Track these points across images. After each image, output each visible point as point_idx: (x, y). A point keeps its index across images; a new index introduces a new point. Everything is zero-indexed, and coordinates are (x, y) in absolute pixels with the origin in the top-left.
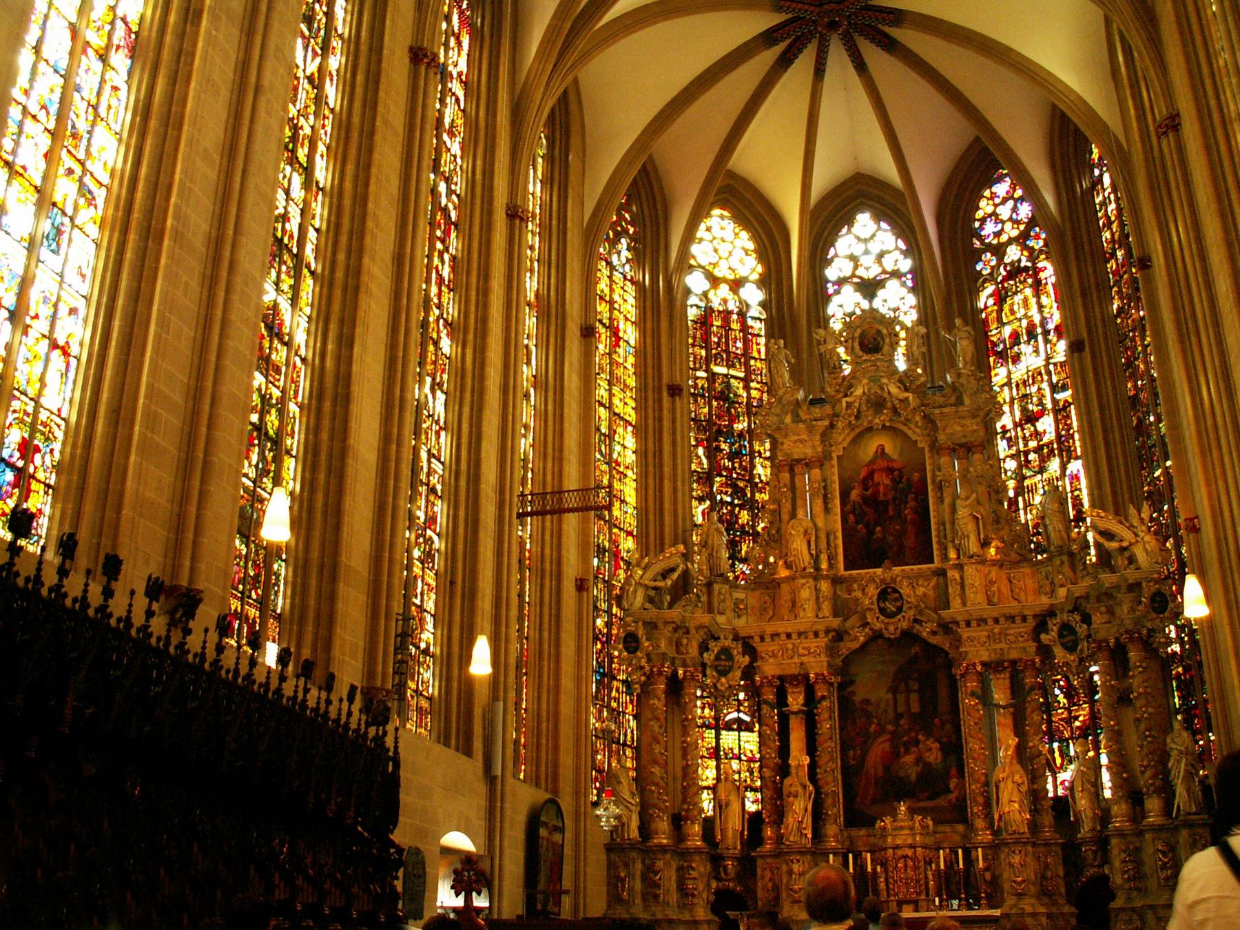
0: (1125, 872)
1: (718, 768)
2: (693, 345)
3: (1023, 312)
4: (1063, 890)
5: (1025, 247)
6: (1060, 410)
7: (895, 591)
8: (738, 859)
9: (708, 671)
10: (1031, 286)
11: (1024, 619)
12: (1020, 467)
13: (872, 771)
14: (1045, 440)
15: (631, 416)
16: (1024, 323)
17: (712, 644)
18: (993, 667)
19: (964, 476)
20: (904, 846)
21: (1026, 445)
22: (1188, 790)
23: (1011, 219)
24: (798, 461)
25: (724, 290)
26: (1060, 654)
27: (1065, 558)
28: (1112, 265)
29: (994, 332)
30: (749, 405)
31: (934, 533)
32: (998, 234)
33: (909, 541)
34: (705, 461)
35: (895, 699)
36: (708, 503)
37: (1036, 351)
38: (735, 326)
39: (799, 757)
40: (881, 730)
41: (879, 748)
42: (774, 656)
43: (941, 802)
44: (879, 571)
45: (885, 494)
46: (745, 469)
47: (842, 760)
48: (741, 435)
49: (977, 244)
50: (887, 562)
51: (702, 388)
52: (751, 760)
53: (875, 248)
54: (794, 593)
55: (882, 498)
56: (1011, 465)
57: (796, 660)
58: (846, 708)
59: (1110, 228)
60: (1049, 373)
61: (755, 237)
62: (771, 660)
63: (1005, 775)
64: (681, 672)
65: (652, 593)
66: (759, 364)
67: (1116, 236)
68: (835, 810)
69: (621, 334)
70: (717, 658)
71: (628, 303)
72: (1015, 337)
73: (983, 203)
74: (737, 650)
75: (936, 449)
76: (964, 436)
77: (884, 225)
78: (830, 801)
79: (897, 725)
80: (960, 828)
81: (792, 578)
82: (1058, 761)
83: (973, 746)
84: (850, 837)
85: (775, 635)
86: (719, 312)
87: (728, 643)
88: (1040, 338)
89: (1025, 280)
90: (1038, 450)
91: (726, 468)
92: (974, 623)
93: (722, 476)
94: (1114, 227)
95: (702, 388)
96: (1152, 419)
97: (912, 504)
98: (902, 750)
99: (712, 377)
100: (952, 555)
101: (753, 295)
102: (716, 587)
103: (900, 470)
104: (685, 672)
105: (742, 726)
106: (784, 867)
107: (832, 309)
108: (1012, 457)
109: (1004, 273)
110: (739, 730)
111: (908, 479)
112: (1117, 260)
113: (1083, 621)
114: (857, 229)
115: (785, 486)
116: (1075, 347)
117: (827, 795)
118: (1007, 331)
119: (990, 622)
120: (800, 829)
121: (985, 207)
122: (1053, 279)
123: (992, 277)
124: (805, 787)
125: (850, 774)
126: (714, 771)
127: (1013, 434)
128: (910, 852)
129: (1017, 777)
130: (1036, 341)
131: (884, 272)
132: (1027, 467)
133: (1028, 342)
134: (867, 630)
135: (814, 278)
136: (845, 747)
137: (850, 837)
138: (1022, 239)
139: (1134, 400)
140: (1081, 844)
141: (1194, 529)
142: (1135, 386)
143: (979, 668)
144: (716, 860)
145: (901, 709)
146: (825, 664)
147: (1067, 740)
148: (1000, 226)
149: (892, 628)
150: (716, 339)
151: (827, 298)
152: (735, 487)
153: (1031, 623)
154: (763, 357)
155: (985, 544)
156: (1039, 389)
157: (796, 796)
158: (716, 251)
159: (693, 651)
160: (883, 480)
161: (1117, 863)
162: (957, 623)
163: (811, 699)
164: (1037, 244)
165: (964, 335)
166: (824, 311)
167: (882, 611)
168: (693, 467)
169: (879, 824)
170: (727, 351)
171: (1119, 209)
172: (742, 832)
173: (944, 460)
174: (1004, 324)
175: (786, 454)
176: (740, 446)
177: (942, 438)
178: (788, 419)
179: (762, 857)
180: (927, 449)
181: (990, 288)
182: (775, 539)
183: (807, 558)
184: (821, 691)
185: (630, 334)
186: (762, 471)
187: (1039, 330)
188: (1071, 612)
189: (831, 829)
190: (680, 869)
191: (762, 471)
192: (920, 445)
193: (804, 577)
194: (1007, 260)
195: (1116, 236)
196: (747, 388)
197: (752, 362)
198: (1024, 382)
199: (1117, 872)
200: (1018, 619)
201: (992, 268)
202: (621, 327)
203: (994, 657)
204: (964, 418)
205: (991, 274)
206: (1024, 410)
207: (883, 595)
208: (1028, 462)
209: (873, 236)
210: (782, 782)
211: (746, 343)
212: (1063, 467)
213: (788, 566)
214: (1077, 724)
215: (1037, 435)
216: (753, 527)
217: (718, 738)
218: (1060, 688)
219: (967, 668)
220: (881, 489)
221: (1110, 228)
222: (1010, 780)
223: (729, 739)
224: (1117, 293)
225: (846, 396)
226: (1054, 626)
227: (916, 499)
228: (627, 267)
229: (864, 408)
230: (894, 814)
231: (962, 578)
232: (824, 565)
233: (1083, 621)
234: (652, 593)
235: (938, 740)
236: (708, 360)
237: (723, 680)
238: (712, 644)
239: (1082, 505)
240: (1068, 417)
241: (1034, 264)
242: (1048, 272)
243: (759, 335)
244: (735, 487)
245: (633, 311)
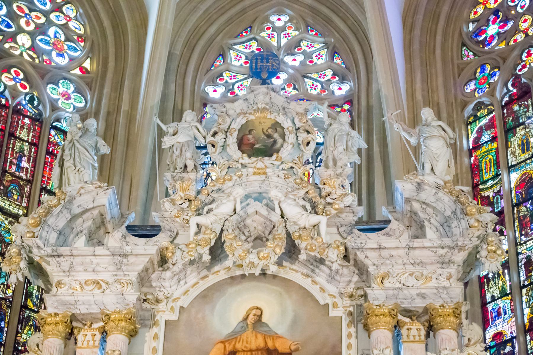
76: (423, 296)
148: (510, 24)
175: (64, 304)
192: (333, 313)
204: (421, 263)
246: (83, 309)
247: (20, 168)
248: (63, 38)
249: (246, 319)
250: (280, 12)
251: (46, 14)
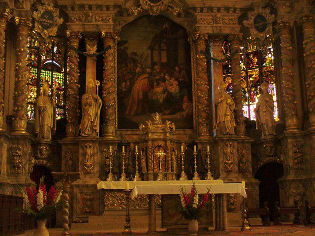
0: (295, 159)
1: (38, 92)
4: (251, 169)
8: (50, 145)
11: (235, 11)
13: (136, 96)
17: (39, 7)
18: (213, 38)
20: (160, 139)
35: (152, 53)
39: (91, 82)
40: (143, 73)
41: (141, 83)
42: (80, 20)
43: (178, 116)
47: (118, 88)
52: (58, 89)
57: (93, 23)
58: (123, 58)
62: (77, 22)
63: (222, 99)
64: (17, 20)
68: (113, 117)
70: (43, 16)
74: (56, 13)
78: (110, 111)
79: (152, 68)
80: (189, 132)
83: (199, 82)
84: (121, 134)
87: (50, 8)
98: (155, 84)
104: (20, 21)
105: (54, 69)
106: (81, 151)
110: (52, 71)
113: (271, 13)
117: (109, 107)
119: (215, 10)
120: (92, 127)
124: (96, 100)
125: (122, 97)
126: (35, 94)
128: (162, 144)
129: (229, 101)
134: (139, 9)
136: (120, 80)
137: (121, 134)
140: (262, 143)
143: (206, 37)
144: (35, 145)
145: (155, 60)
146: (112, 27)
149: (155, 9)
153: (238, 13)
157: (90, 106)
161: (291, 154)
162: (194, 9)
169: (142, 126)
172: (53, 128)
179: (66, 144)
184: (109, 43)
188: (265, 7)
189: (111, 128)
190: (10, 149)
199: (289, 158)
203: (215, 31)
210: (80, 99)
214: (251, 79)
217: (39, 74)
218: (242, 60)
219: (199, 37)
222: (225, 102)
223: (46, 75)
230: (153, 121)
235: (177, 80)
237: (46, 31)
238: (39, 7)
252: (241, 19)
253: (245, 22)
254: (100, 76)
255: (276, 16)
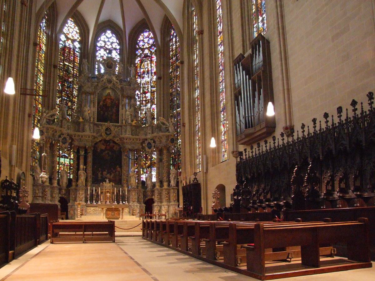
2: (60, 55)
3: (147, 66)
5: (149, 50)
6: (152, 92)
7: (110, 129)
9: (60, 143)
10: (150, 61)
11: (140, 140)
12: (140, 104)
14: (148, 99)
15: (42, 71)
16: (147, 69)
18: (130, 150)
19: (129, 104)
21: (143, 99)
22: (174, 181)
23: (147, 43)
24: (88, 92)
25: (70, 42)
26: (147, 148)
27: (151, 127)
28: (171, 61)
29: (138, 70)
30: (73, 74)
31: (120, 115)
32: (143, 46)
33: (114, 117)
34: (61, 87)
36: (61, 99)
37: (149, 77)
38: (71, 52)
39: (82, 166)
44: (106, 123)
45: (109, 105)
46: (71, 91)
48: (70, 82)
49: (137, 47)
50: (109, 121)
51: (62, 67)
53: (111, 41)
54: (84, 125)
55: (108, 105)
56: (138, 103)
59: (173, 52)
60: (151, 83)
61: (79, 29)
65: (48, 120)
66: (77, 64)
67: (174, 54)
69: (41, 47)
71: (44, 39)
72: (144, 72)
73: (141, 37)
75: (123, 96)
77: (114, 35)
81: (84, 122)
82: (142, 173)
85: (79, 136)
86: (68, 47)
87: (65, 136)
88: (150, 74)
89: (148, 59)
90: (146, 101)
91: (66, 90)
92: (128, 139)
93: (65, 92)
94: (174, 52)
95: (62, 67)
96: (175, 99)
97: (115, 108)
99: (65, 65)
100: (124, 122)
101: (77, 45)
102: (64, 121)
103: (113, 99)
104: (55, 142)
107: (97, 54)
108: (139, 101)
109: (143, 56)
111: (115, 102)
112: (173, 60)
114: (107, 34)
115: (84, 98)
116: (159, 78)
118: (142, 70)
121: (141, 38)
122: (156, 60)
123: (140, 56)
127: (140, 96)
130: (149, 74)
131: (112, 48)
132: (142, 104)
133: (147, 74)
135: (94, 44)
138: (149, 48)
139: (171, 94)
141: (184, 126)
142: (172, 91)
147: (144, 168)
150: (66, 55)
151: (97, 51)
152: (68, 95)
153: (141, 141)
154: (78, 63)
155: (132, 121)
156: (148, 86)
158: (69, 30)
159: (57, 136)
160: (109, 101)
163: (86, 152)
164: (153, 51)
165: (133, 69)
166: (96, 55)
167: (106, 133)
168: (57, 88)
170: (69, 59)
171: (176, 48)
173: (125, 99)
174: (141, 69)
176: (70, 85)
177: (125, 93)
178: (86, 81)
180: (120, 96)
181: (139, 59)
182: (80, 111)
183: (89, 118)
185: (44, 48)
186: (75, 93)
187: (150, 72)
191: (75, 93)
193: (87, 122)
194: (145, 53)
195: (174, 54)
196: (73, 70)
197: (75, 63)
198: (144, 84)
200: (138, 140)
201: (140, 54)
202: (42, 45)
205: (140, 55)
206: (143, 90)
207: (107, 129)
208: (142, 103)
209: (111, 37)
211: (74, 57)
212: (151, 106)
213: (83, 119)
214: (147, 165)
215: (146, 97)
216: (72, 107)
220: (108, 103)
221: (173, 52)
224: (172, 68)
225: (102, 78)
226: (146, 142)
227: (116, 107)
228: (44, 28)
229: (106, 82)
231: (126, 128)
232: (92, 120)
233: (153, 142)
234: (48, 120)
236: (64, 60)
237: (64, 145)
238: (62, 136)
239: (154, 115)
240: (154, 94)
241: (151, 55)
242: (154, 58)
243: (78, 57)
244: (68, 95)
245: (45, 41)
246: (87, 91)
247: (72, 59)
248: (76, 33)
249: (108, 94)
250: (109, 30)
251: (73, 29)
252: (142, 144)
253: (144, 145)
254: (85, 164)
255: (155, 144)
